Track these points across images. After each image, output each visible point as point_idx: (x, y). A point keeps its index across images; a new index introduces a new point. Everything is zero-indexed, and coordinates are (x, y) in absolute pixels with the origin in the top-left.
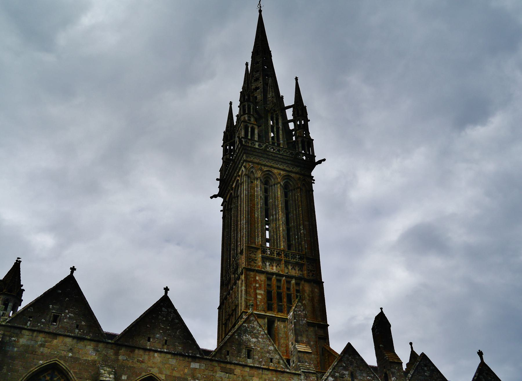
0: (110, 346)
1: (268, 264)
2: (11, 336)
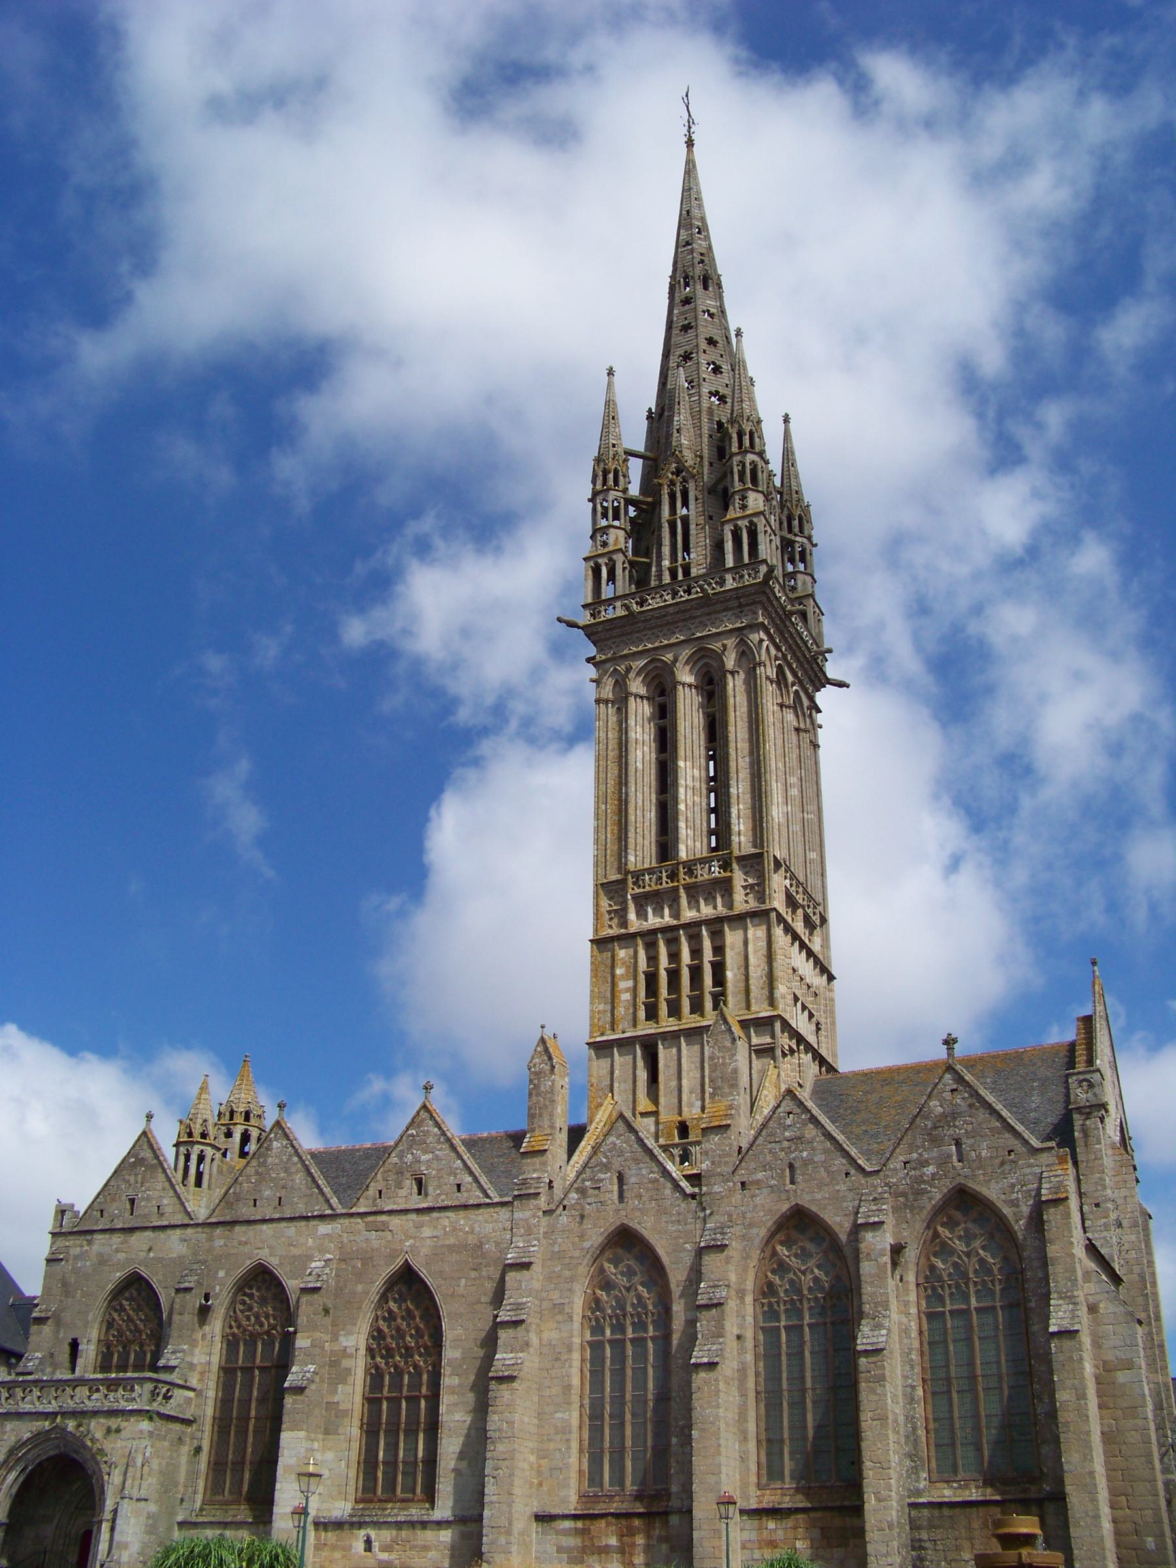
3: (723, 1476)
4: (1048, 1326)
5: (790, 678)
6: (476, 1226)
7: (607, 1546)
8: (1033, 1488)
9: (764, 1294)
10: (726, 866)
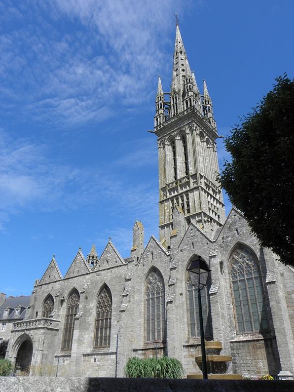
1: (172, 193)
3: (175, 335)
4: (265, 281)
5: (205, 135)
8: (268, 335)
9: (188, 281)
10: (188, 178)
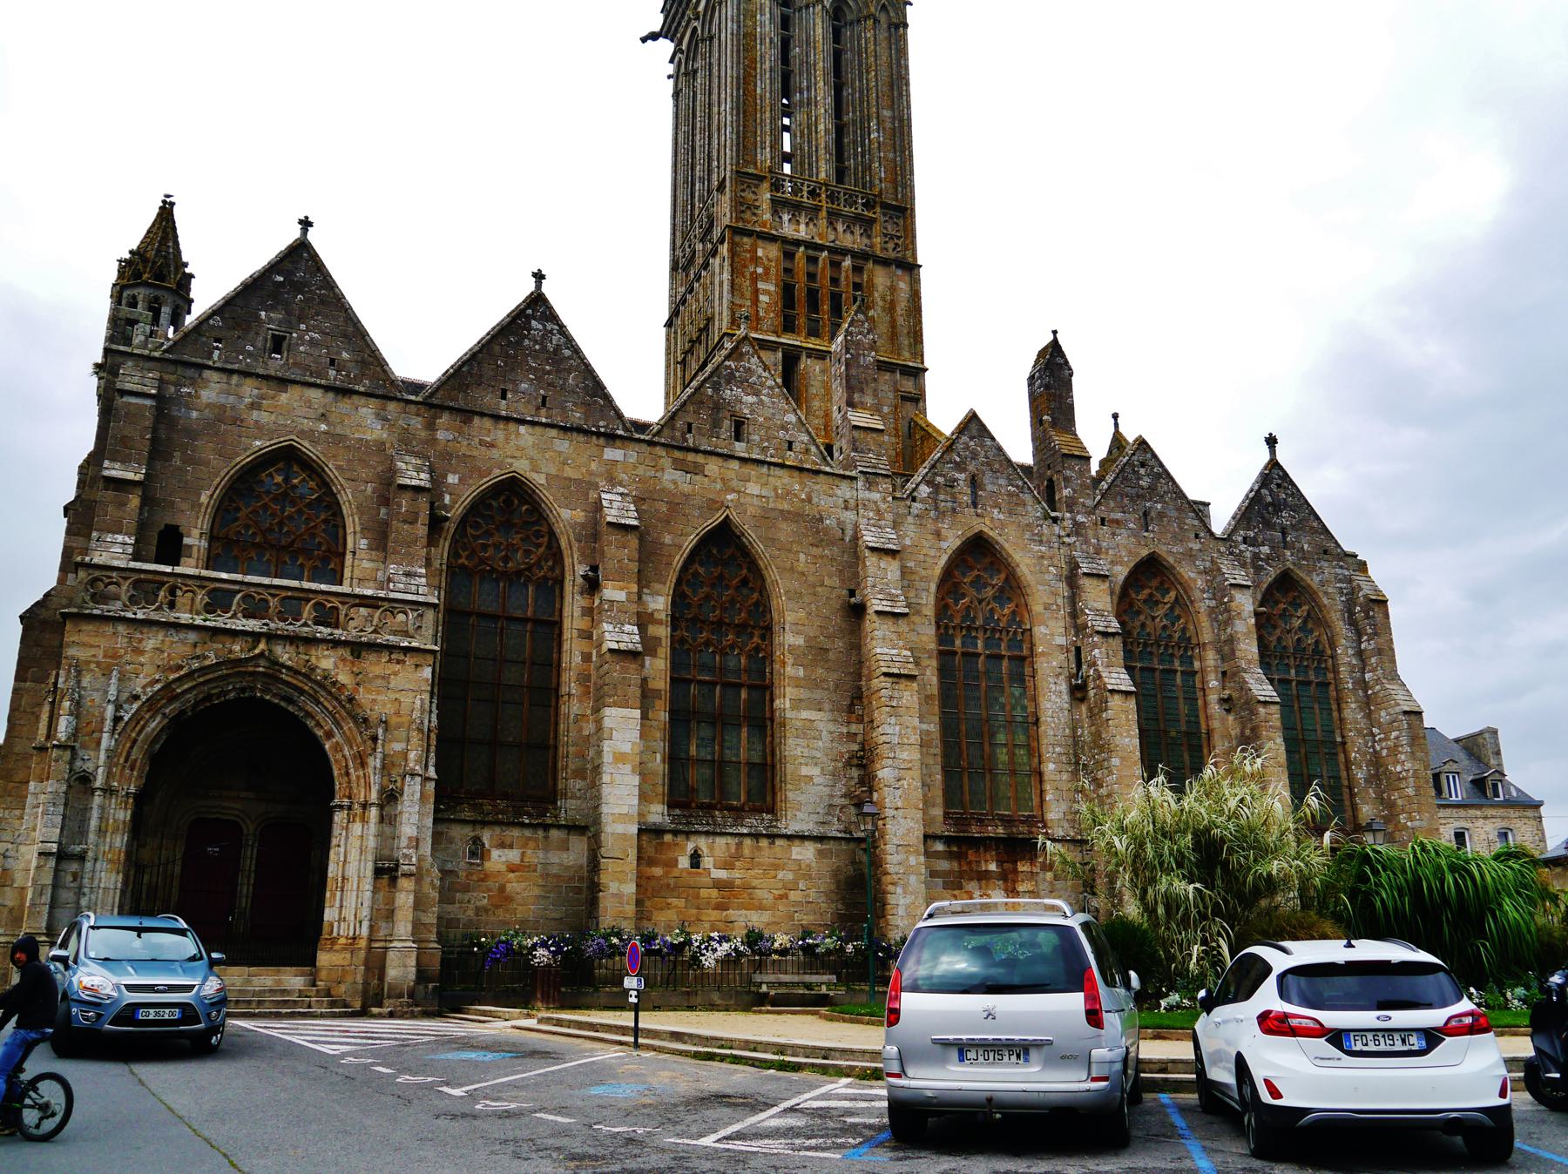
0: (413, 408)
1: (786, 217)
2: (178, 385)
6: (814, 495)
7: (987, 871)
